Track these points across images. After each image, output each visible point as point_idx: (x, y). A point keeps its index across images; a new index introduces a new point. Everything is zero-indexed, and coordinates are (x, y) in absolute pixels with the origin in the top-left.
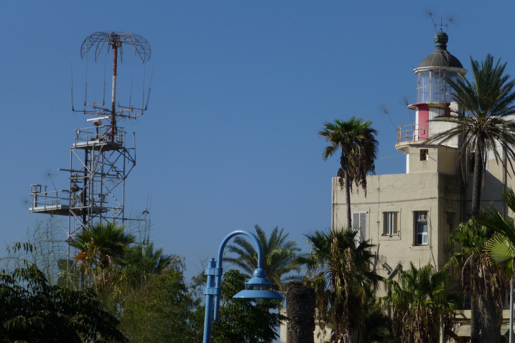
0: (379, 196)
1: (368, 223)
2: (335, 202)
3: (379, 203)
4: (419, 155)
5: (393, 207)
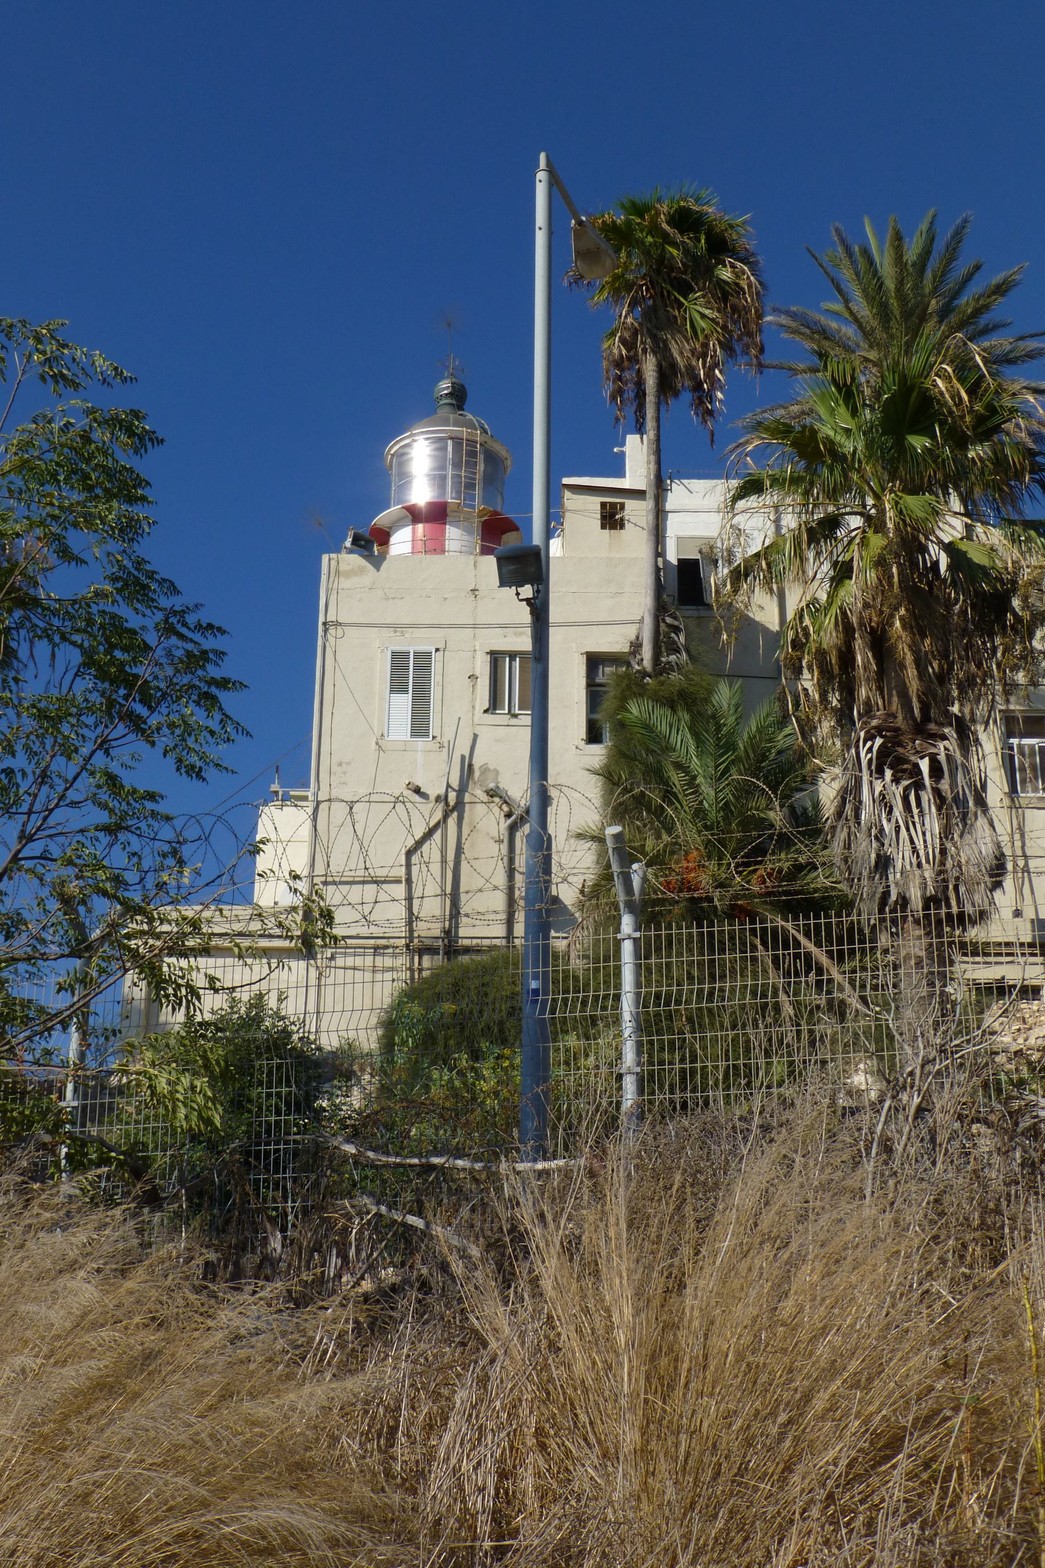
1: (439, 678)
3: (475, 626)
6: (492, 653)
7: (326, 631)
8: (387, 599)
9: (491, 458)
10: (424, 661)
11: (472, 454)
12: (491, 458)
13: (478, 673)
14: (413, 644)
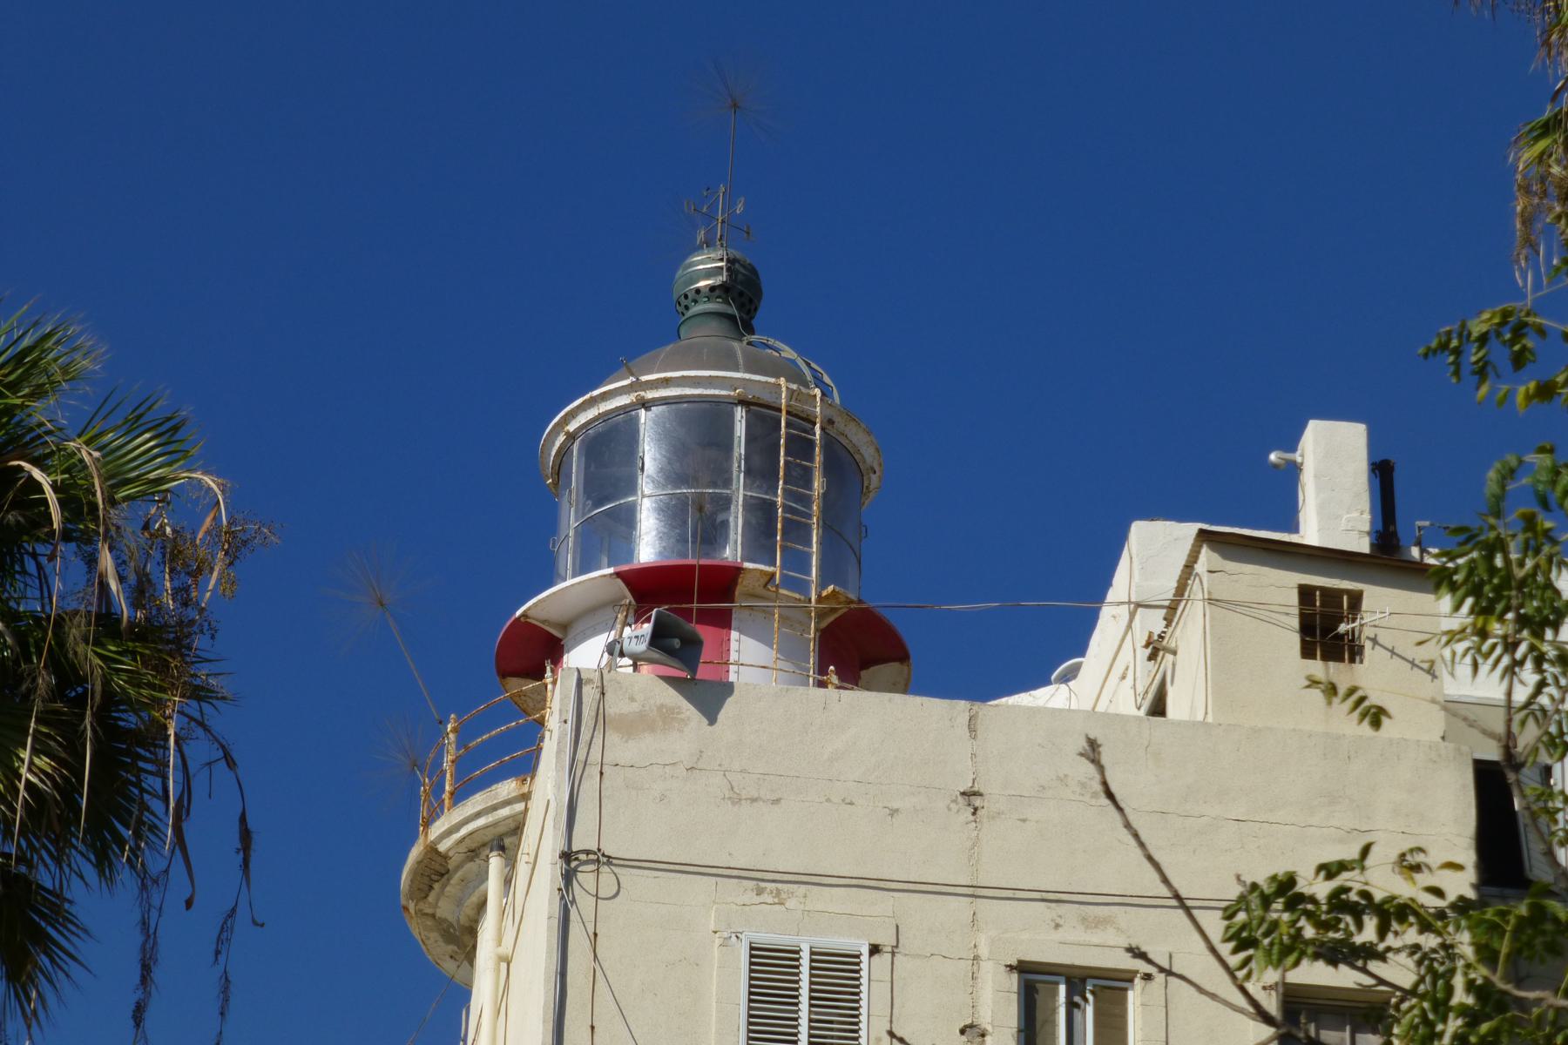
0: (976, 842)
2: (583, 840)
3: (974, 892)
4: (1295, 622)
5: (1095, 937)
6: (1024, 969)
7: (569, 877)
8: (736, 801)
9: (841, 464)
10: (838, 976)
11: (800, 447)
12: (841, 464)
13: (985, 1021)
14: (811, 926)
